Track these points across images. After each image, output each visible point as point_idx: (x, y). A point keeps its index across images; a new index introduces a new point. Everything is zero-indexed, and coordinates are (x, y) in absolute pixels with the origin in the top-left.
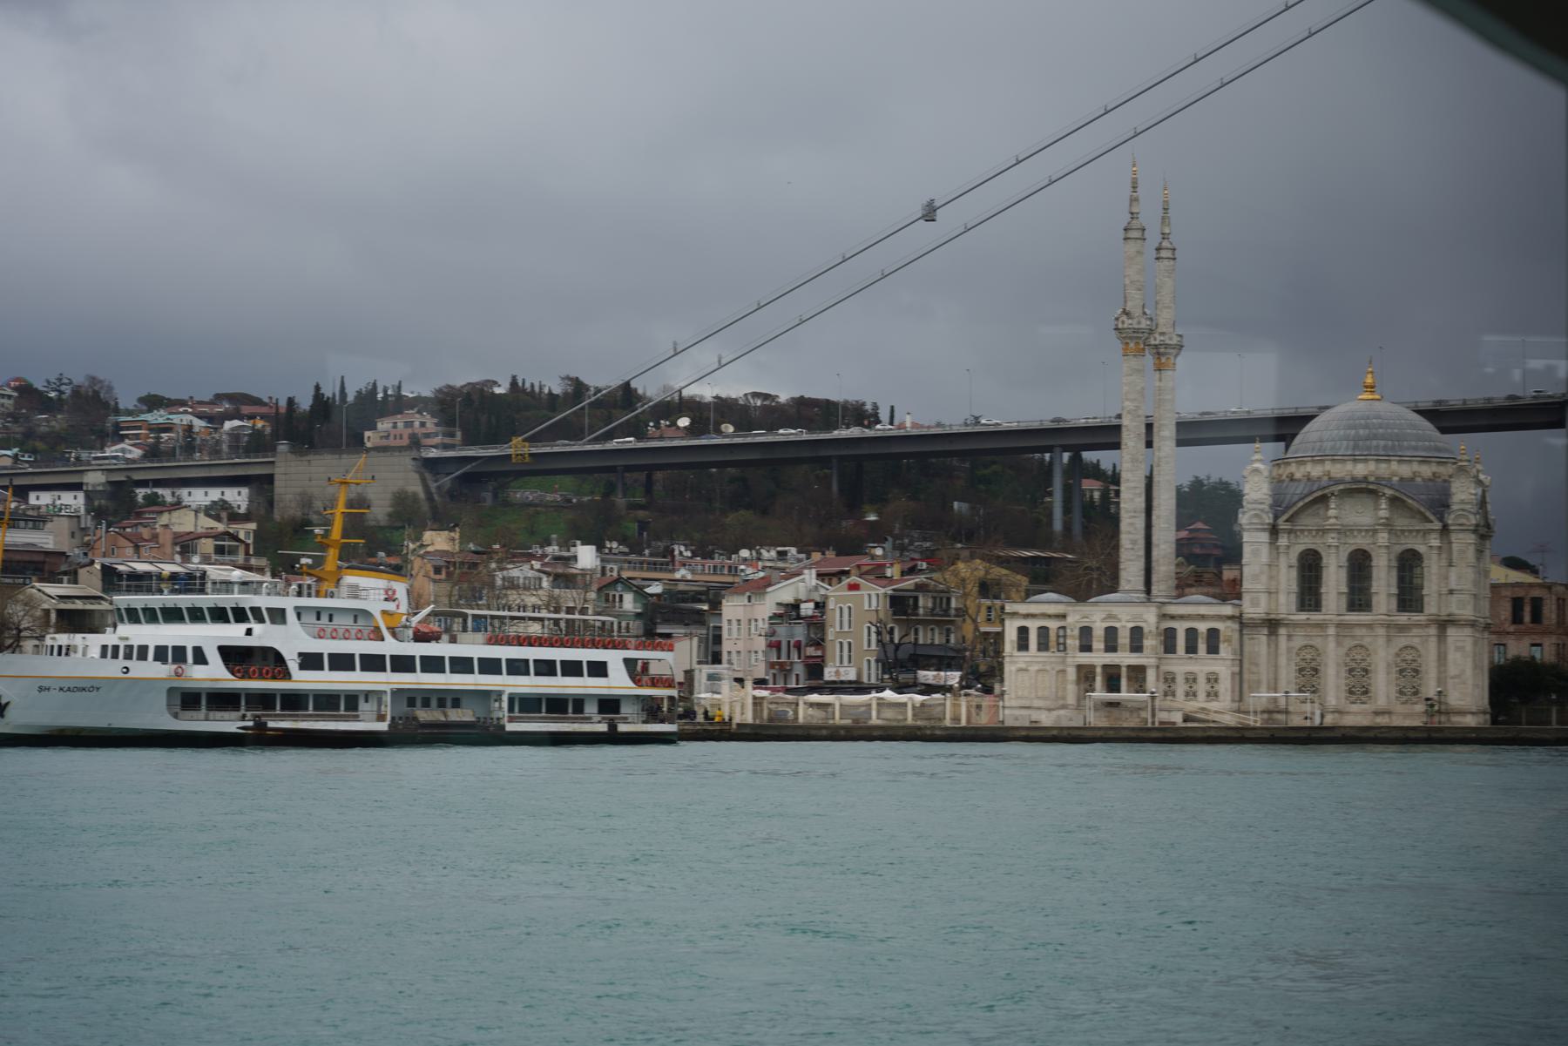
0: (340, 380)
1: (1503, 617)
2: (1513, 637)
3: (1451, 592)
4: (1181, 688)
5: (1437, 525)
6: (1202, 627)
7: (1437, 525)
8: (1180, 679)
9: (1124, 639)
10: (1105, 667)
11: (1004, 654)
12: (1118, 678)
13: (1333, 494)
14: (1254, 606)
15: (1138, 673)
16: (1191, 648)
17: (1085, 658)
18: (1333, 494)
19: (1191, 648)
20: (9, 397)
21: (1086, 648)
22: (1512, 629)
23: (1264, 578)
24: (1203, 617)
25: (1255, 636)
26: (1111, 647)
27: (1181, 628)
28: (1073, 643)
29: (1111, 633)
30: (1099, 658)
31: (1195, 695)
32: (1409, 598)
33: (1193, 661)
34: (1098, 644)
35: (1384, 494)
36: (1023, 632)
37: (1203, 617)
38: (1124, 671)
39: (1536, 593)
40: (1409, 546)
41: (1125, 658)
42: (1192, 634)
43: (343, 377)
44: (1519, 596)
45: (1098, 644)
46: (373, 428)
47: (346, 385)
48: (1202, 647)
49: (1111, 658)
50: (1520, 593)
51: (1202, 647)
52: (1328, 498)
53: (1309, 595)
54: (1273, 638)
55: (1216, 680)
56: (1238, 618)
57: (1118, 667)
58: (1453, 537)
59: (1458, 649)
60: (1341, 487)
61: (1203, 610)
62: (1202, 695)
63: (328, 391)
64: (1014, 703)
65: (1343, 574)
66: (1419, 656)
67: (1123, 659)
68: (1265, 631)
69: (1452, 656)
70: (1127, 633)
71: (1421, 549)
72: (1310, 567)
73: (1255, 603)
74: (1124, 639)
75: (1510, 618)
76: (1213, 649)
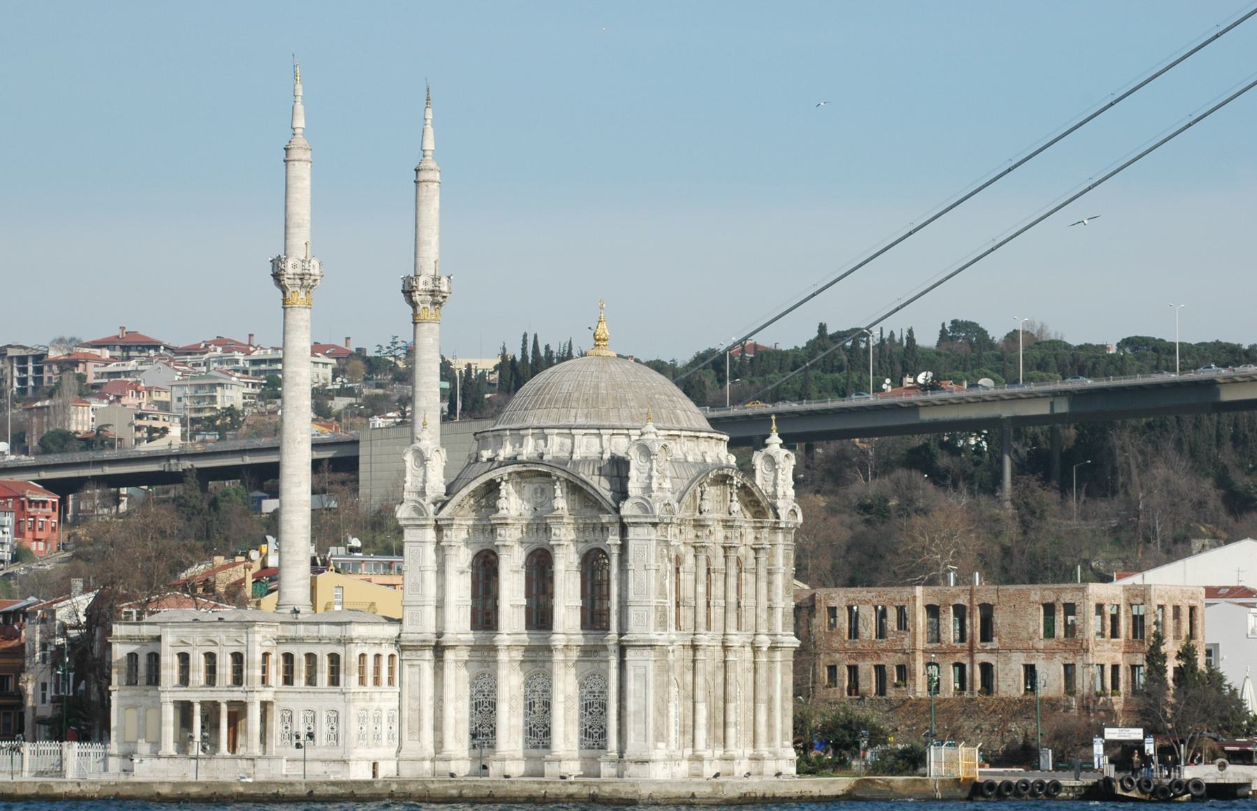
1: (1031, 630)
2: (1043, 655)
6: (322, 653)
10: (202, 703)
11: (110, 688)
13: (502, 479)
14: (423, 625)
15: (238, 712)
16: (311, 680)
17: (183, 695)
19: (311, 680)
20: (325, 364)
21: (184, 680)
24: (320, 641)
25: (415, 663)
30: (197, 694)
33: (312, 695)
34: (198, 674)
37: (320, 641)
38: (224, 709)
41: (224, 694)
42: (311, 658)
43: (536, 337)
44: (1050, 601)
45: (198, 674)
47: (572, 343)
48: (323, 676)
49: (209, 696)
51: (323, 676)
55: (337, 719)
56: (397, 641)
58: (632, 532)
62: (321, 738)
63: (515, 352)
65: (466, 581)
68: (429, 655)
76: (334, 681)
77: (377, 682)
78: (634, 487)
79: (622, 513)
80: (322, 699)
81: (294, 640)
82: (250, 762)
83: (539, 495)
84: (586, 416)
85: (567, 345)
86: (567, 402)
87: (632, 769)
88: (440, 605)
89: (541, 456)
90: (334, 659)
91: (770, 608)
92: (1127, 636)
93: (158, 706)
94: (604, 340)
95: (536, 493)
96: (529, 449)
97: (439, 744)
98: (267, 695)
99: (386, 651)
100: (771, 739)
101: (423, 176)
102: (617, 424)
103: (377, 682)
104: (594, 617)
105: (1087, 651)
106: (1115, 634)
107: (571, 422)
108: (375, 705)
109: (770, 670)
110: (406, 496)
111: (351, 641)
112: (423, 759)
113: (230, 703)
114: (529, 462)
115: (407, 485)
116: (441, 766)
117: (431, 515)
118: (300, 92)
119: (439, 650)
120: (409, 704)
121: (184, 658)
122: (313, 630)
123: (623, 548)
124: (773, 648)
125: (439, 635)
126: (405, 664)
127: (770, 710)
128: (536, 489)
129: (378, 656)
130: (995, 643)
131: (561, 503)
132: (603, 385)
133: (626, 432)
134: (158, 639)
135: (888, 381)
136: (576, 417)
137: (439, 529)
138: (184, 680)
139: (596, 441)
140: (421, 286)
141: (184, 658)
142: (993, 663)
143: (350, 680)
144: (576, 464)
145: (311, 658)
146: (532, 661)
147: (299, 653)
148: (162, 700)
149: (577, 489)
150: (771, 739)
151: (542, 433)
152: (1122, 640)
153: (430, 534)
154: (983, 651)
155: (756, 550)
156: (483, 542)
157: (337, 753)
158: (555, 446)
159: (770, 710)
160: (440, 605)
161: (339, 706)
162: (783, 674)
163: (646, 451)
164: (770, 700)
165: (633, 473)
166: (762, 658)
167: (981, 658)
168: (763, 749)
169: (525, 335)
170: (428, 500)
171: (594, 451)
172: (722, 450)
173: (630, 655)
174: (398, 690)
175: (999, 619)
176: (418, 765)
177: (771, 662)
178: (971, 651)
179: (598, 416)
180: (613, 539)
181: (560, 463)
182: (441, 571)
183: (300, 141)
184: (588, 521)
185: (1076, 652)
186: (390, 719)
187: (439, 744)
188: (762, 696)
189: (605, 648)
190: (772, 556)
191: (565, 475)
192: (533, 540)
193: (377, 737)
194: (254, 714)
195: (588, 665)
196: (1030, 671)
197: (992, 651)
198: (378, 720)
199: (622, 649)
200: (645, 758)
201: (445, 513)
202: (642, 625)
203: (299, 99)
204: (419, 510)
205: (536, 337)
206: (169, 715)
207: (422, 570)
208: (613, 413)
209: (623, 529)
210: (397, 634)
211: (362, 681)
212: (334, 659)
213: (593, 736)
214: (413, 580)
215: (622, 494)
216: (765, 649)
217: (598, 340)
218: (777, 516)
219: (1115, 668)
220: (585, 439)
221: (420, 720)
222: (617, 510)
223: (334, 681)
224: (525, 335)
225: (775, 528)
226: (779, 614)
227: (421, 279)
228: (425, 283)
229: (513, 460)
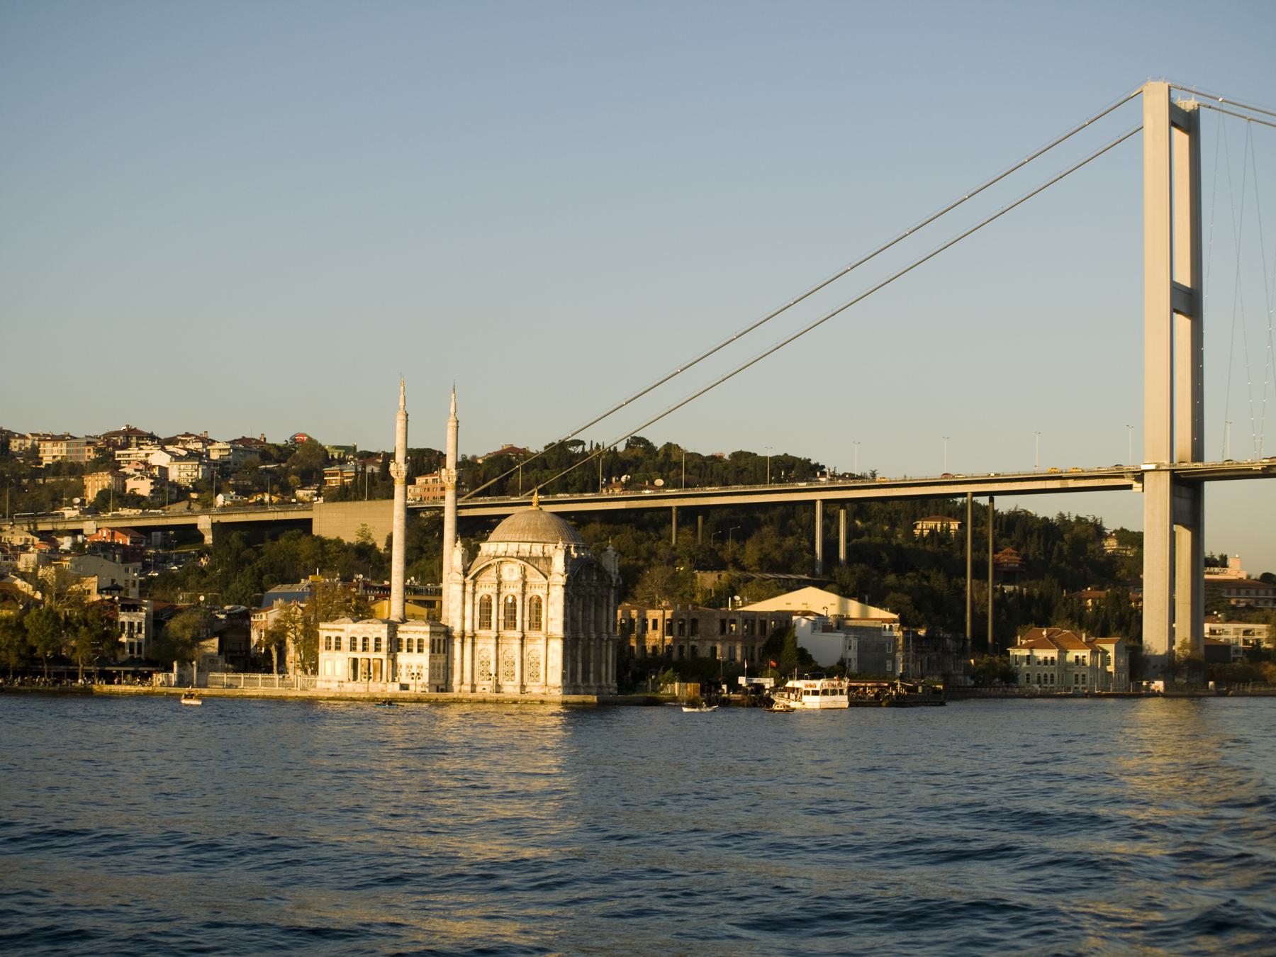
3: (551, 619)
7: (546, 582)
17: (353, 655)
21: (353, 648)
22: (719, 638)
23: (459, 611)
28: (345, 643)
32: (536, 624)
34: (359, 647)
41: (372, 655)
45: (359, 647)
46: (414, 483)
48: (415, 649)
50: (724, 617)
53: (485, 622)
59: (553, 652)
60: (499, 560)
64: (323, 678)
70: (374, 641)
72: (486, 606)
75: (719, 632)
76: (420, 651)
77: (439, 652)
100: (607, 679)
103: (439, 652)
108: (438, 661)
109: (607, 649)
124: (609, 639)
129: (439, 640)
138: (353, 648)
154: (693, 640)
162: (613, 650)
164: (607, 662)
167: (692, 643)
168: (604, 683)
175: (700, 625)
186: (444, 668)
193: (439, 675)
196: (714, 650)
197: (696, 640)
198: (439, 668)
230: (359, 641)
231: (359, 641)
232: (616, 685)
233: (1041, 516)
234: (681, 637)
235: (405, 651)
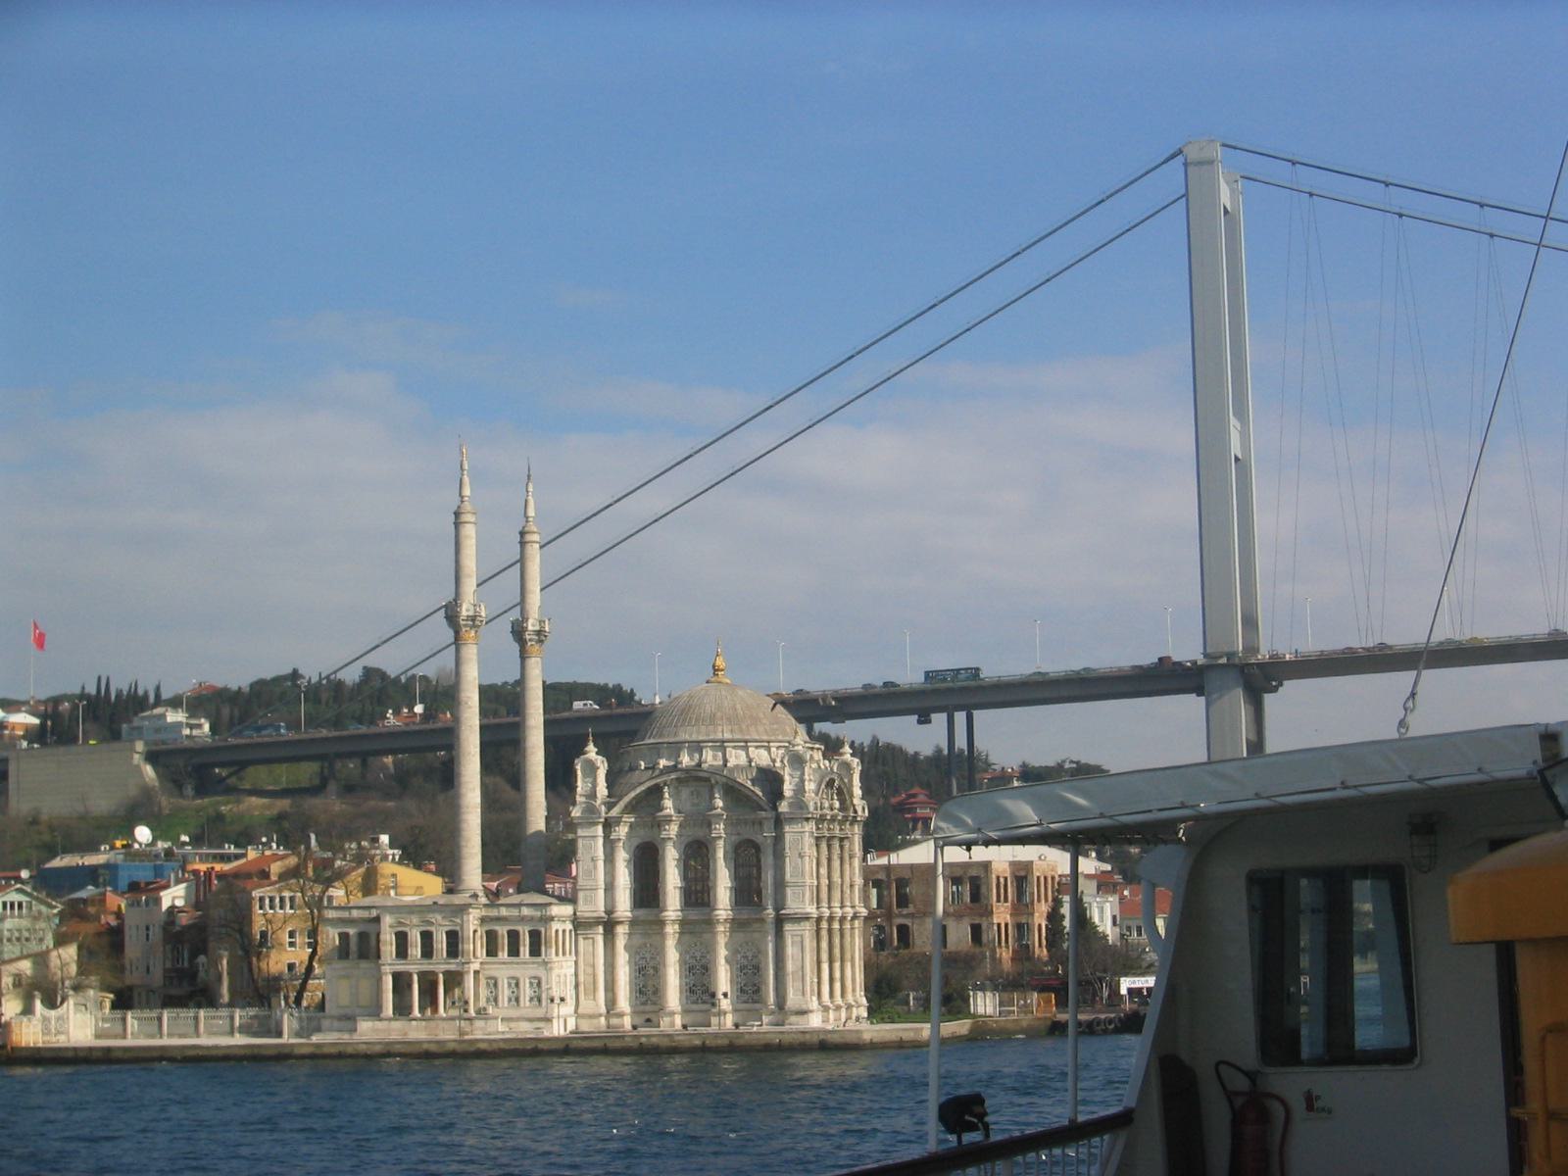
0: (96, 680)
4: (505, 993)
5: (771, 814)
8: (503, 984)
9: (441, 942)
12: (434, 985)
14: (593, 905)
15: (454, 980)
16: (514, 951)
18: (665, 784)
21: (402, 952)
24: (522, 919)
26: (428, 951)
27: (502, 930)
29: (427, 938)
31: (517, 1000)
34: (415, 951)
35: (717, 783)
36: (344, 937)
39: (974, 873)
40: (746, 836)
41: (440, 964)
42: (514, 936)
43: (108, 679)
44: (958, 875)
45: (415, 951)
50: (958, 873)
52: (662, 788)
54: (609, 936)
57: (434, 974)
61: (526, 911)
62: (525, 1001)
66: (759, 952)
67: (437, 966)
68: (601, 929)
69: (790, 950)
71: (759, 839)
73: (589, 901)
74: (441, 942)
76: (535, 951)
77: (564, 954)
78: (788, 789)
79: (780, 810)
80: (524, 968)
81: (499, 919)
82: (467, 1022)
83: (695, 796)
84: (732, 731)
85: (133, 685)
86: (712, 720)
87: (793, 1019)
88: (610, 888)
89: (699, 765)
90: (535, 936)
91: (852, 886)
92: (1013, 901)
93: (379, 980)
94: (722, 670)
95: (692, 795)
96: (686, 760)
97: (611, 1002)
98: (475, 966)
99: (569, 926)
100: (854, 990)
101: (528, 538)
102: (757, 737)
103: (564, 954)
104: (747, 893)
105: (992, 913)
106: (1006, 900)
107: (719, 736)
109: (852, 936)
110: (579, 799)
111: (552, 919)
112: (600, 1015)
113: (447, 974)
114: (687, 770)
115: (579, 789)
116: (614, 1021)
117: (603, 815)
118: (466, 467)
119: (609, 925)
120: (584, 971)
121: (402, 939)
122: (515, 912)
123: (779, 839)
125: (610, 911)
126: (580, 938)
127: (853, 966)
128: (692, 792)
129: (564, 931)
130: (911, 909)
131: (719, 803)
132: (738, 706)
133: (766, 744)
134: (377, 920)
135: (390, 711)
136: (723, 732)
137: (608, 825)
138: (402, 952)
139: (743, 753)
140: (530, 628)
141: (402, 939)
142: (910, 924)
143: (550, 953)
144: (732, 770)
145: (514, 936)
146: (691, 933)
147: (502, 930)
148: (383, 971)
149: (733, 791)
150: (854, 990)
151: (697, 747)
152: (1009, 904)
153: (600, 828)
155: (842, 840)
156: (644, 835)
157: (540, 1013)
158: (710, 758)
159: (853, 966)
160: (610, 888)
161: (541, 973)
163: (797, 761)
165: (787, 778)
166: (847, 926)
168: (850, 998)
169: (99, 679)
170: (599, 802)
171: (743, 760)
172: (818, 756)
173: (788, 927)
174: (575, 958)
176: (595, 1021)
177: (852, 929)
178: (889, 916)
179: (741, 731)
180: (769, 834)
181: (715, 771)
182: (610, 859)
183: (467, 506)
184: (741, 817)
185: (981, 916)
187: (611, 1002)
188: (848, 956)
189: (762, 921)
190: (852, 843)
191: (724, 780)
192: (690, 833)
194: (469, 981)
195: (741, 935)
199: (780, 921)
200: (804, 1007)
201: (615, 812)
202: (799, 901)
203: (465, 472)
204: (591, 810)
205: (108, 679)
206: (388, 983)
207: (594, 860)
208: (752, 729)
209: (779, 822)
210: (572, 913)
211: (557, 954)
212: (535, 936)
213: (749, 989)
214: (586, 867)
215: (776, 794)
216: (849, 918)
217: (718, 670)
218: (855, 812)
219: (1006, 925)
220: (734, 751)
221: (595, 982)
222: (775, 808)
223: (535, 951)
224: (99, 679)
225: (854, 821)
226: (856, 889)
227: (530, 622)
228: (533, 625)
229: (674, 768)
230: (415, 937)
231: (415, 937)
232: (864, 1001)
233: (911, 751)
234: (878, 912)
235: (503, 955)
